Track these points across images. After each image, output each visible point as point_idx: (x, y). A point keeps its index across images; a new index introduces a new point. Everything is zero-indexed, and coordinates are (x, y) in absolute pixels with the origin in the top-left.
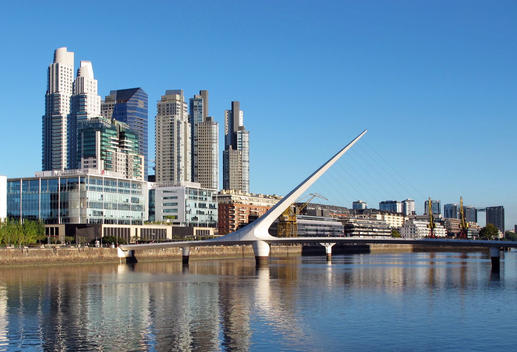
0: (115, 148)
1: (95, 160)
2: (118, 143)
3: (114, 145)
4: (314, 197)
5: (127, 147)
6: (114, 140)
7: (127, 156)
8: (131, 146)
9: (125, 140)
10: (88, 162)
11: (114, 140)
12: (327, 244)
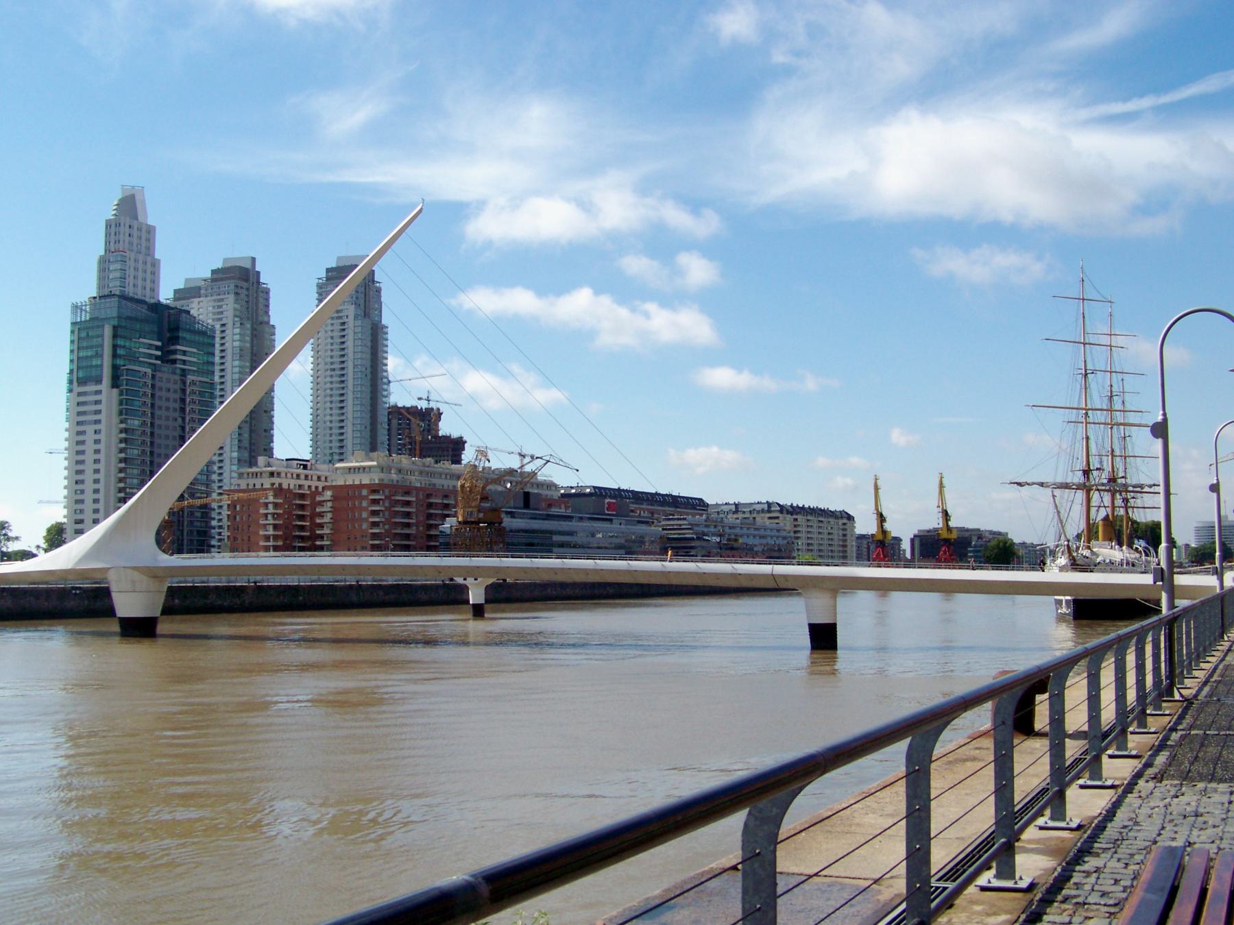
0: (150, 364)
2: (159, 353)
3: (150, 356)
4: (545, 464)
5: (184, 362)
6: (150, 346)
8: (195, 360)
9: (179, 347)
11: (150, 346)
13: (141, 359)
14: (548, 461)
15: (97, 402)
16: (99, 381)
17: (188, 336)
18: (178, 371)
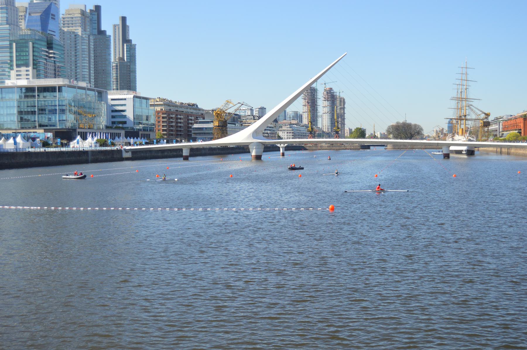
1: (27, 69)
2: (47, 54)
7: (55, 66)
10: (20, 71)
12: (282, 145)
13: (43, 57)
14: (242, 104)
15: (27, 75)
16: (27, 65)
17: (57, 47)
18: (53, 62)
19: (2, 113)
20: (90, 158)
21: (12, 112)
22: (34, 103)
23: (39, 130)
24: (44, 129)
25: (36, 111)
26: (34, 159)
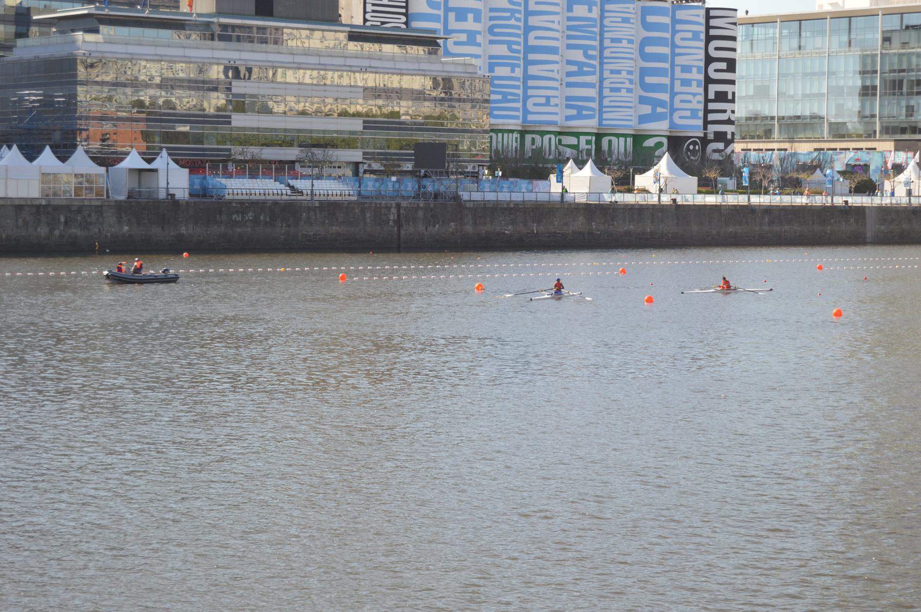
19: (792, 93)
20: (871, 227)
21: (815, 90)
22: (874, 63)
23: (881, 143)
24: (895, 140)
25: (876, 87)
26: (623, 227)
